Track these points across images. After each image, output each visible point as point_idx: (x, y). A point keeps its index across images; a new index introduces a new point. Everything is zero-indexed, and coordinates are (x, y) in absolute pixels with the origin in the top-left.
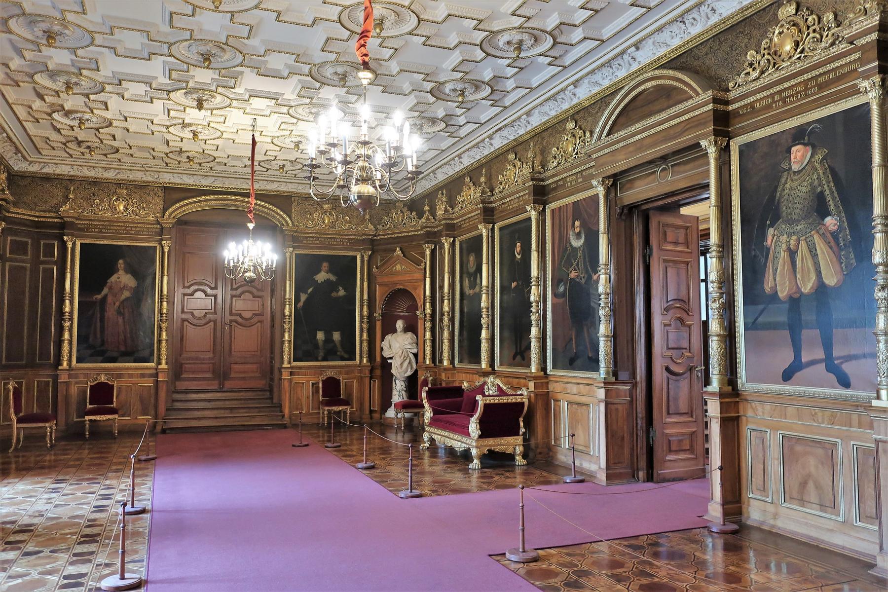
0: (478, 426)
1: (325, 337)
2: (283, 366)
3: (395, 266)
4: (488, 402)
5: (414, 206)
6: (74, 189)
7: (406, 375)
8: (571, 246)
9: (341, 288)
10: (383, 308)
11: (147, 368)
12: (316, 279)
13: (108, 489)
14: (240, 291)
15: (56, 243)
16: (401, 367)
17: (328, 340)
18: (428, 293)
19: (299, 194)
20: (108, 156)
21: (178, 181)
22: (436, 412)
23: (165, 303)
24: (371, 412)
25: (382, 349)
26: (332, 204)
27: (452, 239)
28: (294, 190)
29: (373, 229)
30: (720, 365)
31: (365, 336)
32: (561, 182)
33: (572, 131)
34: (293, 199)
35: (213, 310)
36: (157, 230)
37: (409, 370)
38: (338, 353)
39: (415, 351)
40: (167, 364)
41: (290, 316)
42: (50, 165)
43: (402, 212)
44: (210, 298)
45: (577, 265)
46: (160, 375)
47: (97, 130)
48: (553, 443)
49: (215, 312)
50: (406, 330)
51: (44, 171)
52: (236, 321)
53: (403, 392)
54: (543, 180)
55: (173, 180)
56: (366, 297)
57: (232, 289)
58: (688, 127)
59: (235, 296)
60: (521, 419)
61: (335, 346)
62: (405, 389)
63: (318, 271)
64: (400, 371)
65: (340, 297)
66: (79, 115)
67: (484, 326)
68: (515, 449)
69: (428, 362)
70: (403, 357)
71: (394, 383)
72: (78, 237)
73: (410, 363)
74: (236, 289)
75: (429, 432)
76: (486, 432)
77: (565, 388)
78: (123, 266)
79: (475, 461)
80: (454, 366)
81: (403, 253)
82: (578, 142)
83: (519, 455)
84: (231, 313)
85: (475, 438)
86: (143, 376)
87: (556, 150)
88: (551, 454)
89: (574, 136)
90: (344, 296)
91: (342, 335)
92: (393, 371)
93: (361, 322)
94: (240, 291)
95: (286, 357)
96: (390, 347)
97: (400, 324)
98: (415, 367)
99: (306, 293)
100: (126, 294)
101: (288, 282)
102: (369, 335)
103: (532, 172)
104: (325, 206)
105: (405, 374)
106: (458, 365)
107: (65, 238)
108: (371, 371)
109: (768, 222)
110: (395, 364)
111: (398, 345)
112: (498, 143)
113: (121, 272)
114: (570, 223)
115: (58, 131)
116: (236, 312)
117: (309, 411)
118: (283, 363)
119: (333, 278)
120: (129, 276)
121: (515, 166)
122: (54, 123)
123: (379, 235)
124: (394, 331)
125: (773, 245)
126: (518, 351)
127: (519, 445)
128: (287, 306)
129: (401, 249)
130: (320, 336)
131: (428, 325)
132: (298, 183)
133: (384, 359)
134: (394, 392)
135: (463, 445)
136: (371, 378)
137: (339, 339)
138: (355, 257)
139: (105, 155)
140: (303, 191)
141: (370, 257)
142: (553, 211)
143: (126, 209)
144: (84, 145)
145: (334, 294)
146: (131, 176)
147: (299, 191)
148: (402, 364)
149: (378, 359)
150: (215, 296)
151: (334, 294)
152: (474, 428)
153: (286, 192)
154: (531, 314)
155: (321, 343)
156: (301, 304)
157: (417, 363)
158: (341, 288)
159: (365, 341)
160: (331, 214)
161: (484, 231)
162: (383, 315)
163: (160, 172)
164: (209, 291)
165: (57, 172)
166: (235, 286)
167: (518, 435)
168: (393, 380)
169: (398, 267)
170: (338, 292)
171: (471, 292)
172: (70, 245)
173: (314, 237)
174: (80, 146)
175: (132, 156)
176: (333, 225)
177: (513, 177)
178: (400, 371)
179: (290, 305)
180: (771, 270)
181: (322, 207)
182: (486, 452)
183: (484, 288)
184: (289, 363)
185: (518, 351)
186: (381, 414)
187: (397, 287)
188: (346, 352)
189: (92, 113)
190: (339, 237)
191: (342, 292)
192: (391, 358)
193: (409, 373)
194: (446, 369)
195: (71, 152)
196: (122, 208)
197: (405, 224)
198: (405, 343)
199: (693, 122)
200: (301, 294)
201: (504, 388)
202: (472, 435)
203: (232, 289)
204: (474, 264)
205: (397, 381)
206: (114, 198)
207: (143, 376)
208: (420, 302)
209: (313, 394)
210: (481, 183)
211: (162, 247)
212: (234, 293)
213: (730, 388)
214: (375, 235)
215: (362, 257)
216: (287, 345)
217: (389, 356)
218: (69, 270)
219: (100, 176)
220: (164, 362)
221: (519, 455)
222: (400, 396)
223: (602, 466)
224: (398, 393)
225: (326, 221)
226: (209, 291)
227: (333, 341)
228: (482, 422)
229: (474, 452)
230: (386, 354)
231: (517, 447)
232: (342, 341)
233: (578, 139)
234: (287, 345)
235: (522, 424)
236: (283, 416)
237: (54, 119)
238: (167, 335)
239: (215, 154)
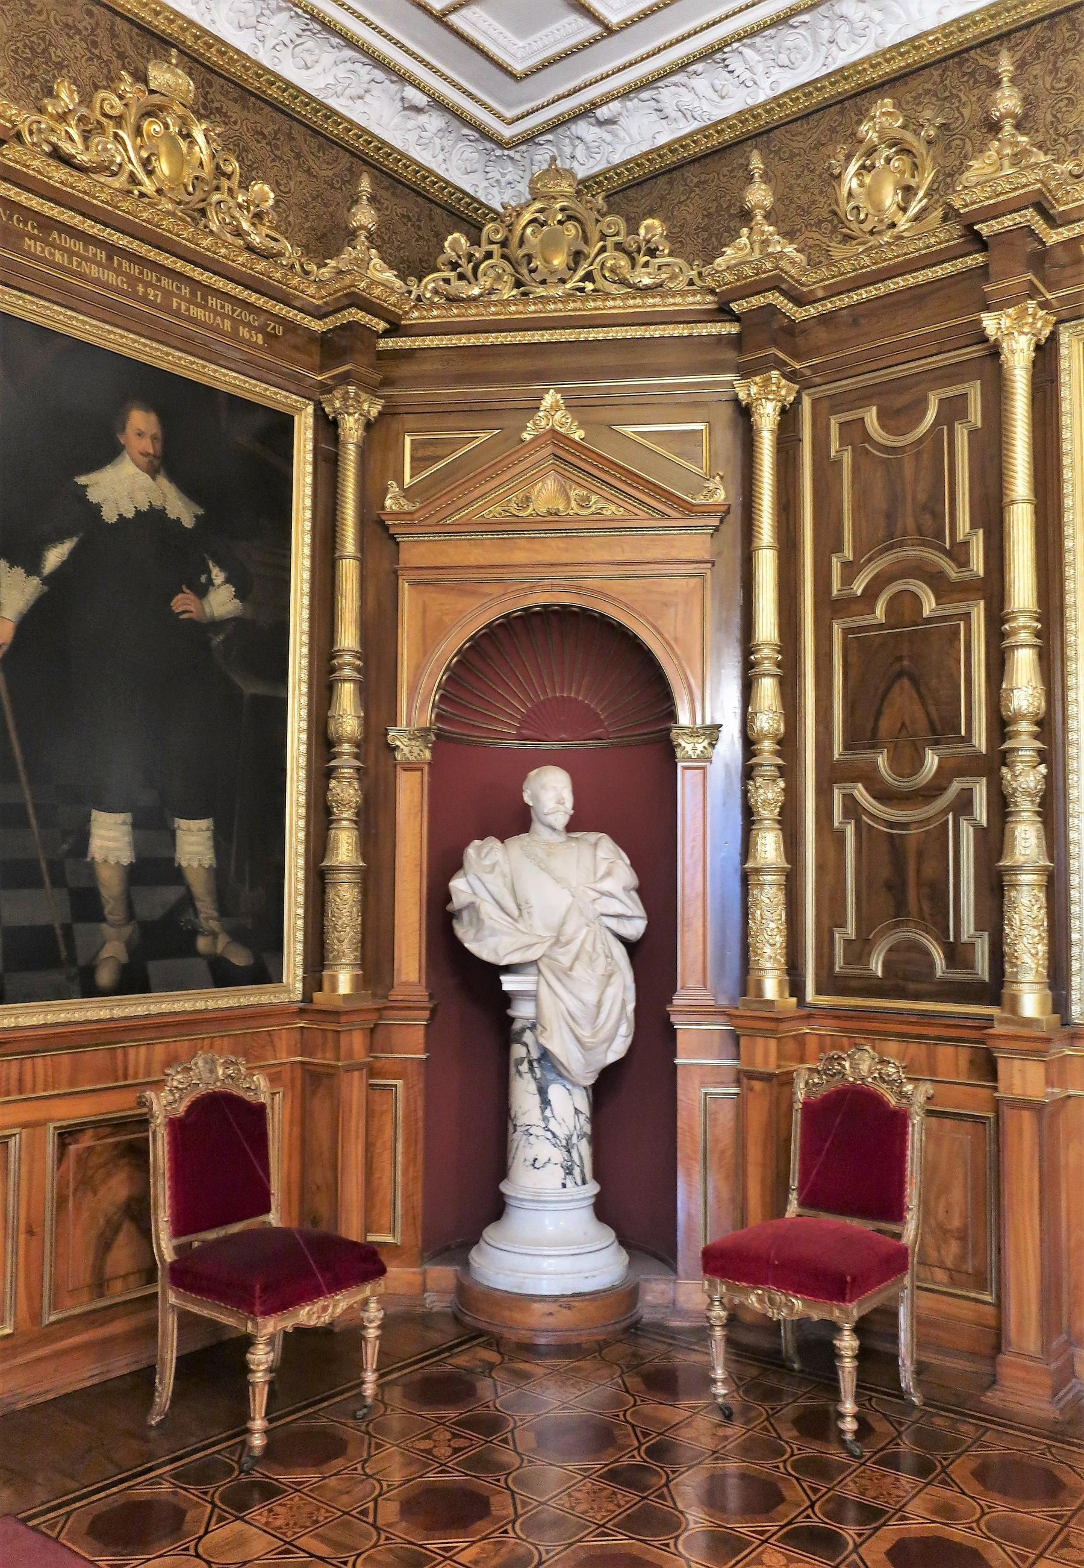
1: (137, 846)
12: (93, 496)
38: (202, 944)
61: (189, 900)
65: (217, 625)
69: (771, 988)
90: (235, 622)
91: (221, 840)
99: (32, 566)
117: (36, 1317)
137: (208, 858)
138: (283, 425)
145: (183, 603)
151: (183, 603)
155: (110, 884)
158: (218, 575)
170: (202, 591)
188: (237, 936)
190: (220, 283)
198: (607, 885)
209: (61, 1202)
222: (569, 1171)
224: (558, 1155)
227: (176, 875)
232: (218, 874)
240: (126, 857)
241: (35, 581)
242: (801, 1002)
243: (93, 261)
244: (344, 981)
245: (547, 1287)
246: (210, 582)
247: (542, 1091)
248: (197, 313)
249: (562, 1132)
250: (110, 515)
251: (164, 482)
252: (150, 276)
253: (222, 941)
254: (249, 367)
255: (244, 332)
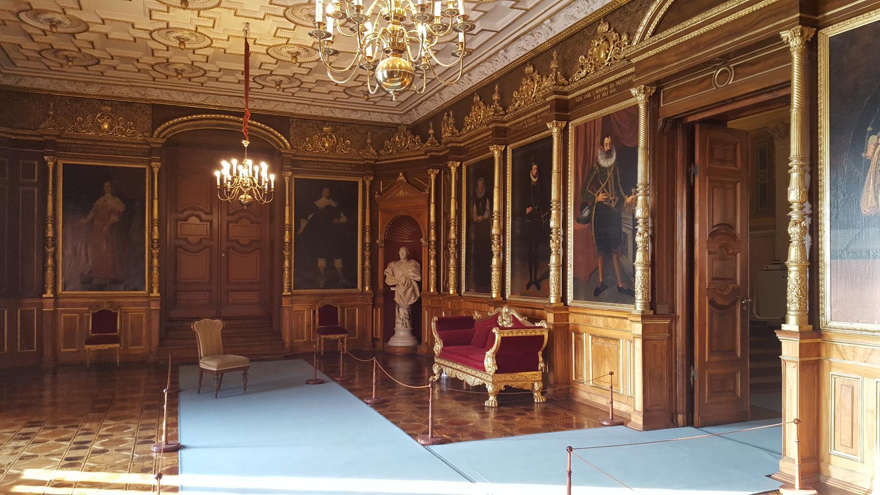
0: (495, 362)
2: (283, 294)
3: (398, 192)
4: (506, 335)
5: (418, 129)
6: (54, 105)
7: (409, 303)
8: (599, 166)
9: (342, 215)
10: (385, 235)
11: (138, 297)
12: (317, 205)
13: (86, 434)
14: (236, 216)
15: (36, 163)
16: (405, 296)
17: (330, 267)
18: (432, 219)
19: (297, 115)
20: (90, 68)
21: (167, 98)
22: (445, 344)
23: (156, 228)
24: (373, 339)
25: (385, 277)
26: (332, 126)
27: (459, 163)
28: (292, 111)
29: (375, 153)
30: (800, 300)
31: (367, 263)
32: (589, 95)
33: (604, 35)
34: (291, 120)
35: (208, 236)
36: (146, 151)
37: (413, 298)
38: (340, 281)
39: (418, 278)
40: (159, 291)
41: (290, 243)
42: (26, 78)
43: (405, 136)
44: (206, 223)
45: (607, 187)
46: (152, 303)
47: (73, 35)
48: (574, 379)
49: (211, 239)
50: (409, 258)
51: (21, 84)
52: (233, 248)
53: (407, 320)
54: (566, 94)
55: (161, 98)
56: (367, 223)
57: (228, 214)
58: (763, 16)
59: (232, 222)
60: (540, 353)
62: (408, 317)
63: (319, 197)
64: (404, 299)
66: (49, 16)
67: (495, 254)
68: (533, 385)
69: (432, 290)
70: (406, 285)
71: (397, 311)
72: (60, 157)
73: (413, 291)
74: (233, 214)
75: (439, 364)
76: (503, 367)
77: (589, 321)
78: (109, 188)
79: (491, 398)
80: (460, 295)
81: (406, 179)
82: (612, 47)
83: (537, 392)
84: (228, 240)
85: (491, 374)
86: (134, 304)
87: (584, 58)
88: (571, 390)
89: (606, 40)
92: (397, 299)
93: (363, 249)
94: (236, 216)
95: (286, 285)
96: (393, 275)
97: (403, 252)
98: (418, 294)
99: (306, 219)
100: (114, 218)
101: (287, 208)
102: (371, 263)
103: (555, 84)
104: (325, 129)
105: (408, 302)
106: (464, 293)
107: (46, 158)
108: (374, 299)
109: (869, 129)
110: (399, 291)
111: (401, 273)
112: (514, 54)
113: (107, 195)
114: (598, 140)
115: (30, 36)
116: (233, 238)
118: (283, 291)
119: (333, 204)
120: (117, 199)
121: (533, 80)
122: (24, 26)
123: (381, 160)
124: (397, 258)
125: (876, 156)
126: (533, 280)
127: (538, 381)
128: (287, 232)
129: (404, 175)
130: (322, 263)
131: (433, 253)
132: (296, 103)
133: (387, 287)
134: (398, 320)
135: (478, 380)
136: (373, 306)
137: (341, 266)
139: (86, 67)
140: (302, 112)
141: (372, 182)
142: (577, 128)
143: (111, 127)
144: (61, 54)
145: (335, 221)
146: (116, 92)
147: (297, 112)
148: (405, 292)
149: (381, 286)
150: (211, 222)
151: (335, 221)
152: (489, 362)
153: (284, 113)
154: (551, 241)
156: (301, 230)
157: (420, 290)
158: (342, 215)
159: (367, 269)
160: (331, 137)
161: (496, 153)
162: (386, 242)
163: (146, 87)
164: (204, 216)
165: (35, 86)
166: (231, 212)
167: (537, 370)
168: (397, 309)
169: (401, 193)
171: (480, 218)
172: (51, 164)
173: (314, 161)
174: (56, 56)
175: (115, 68)
176: (333, 148)
177: (530, 93)
178: (404, 299)
179: (290, 231)
180: (871, 187)
181: (322, 130)
182: (503, 388)
183: (496, 214)
184: (290, 290)
185: (533, 280)
186: (384, 342)
187: (401, 214)
189: (65, 13)
191: (343, 219)
192: (394, 286)
193: (413, 301)
194: (452, 297)
195: (48, 63)
196: (106, 126)
197: (408, 148)
199: (771, 10)
200: (301, 220)
201: (520, 319)
202: (488, 370)
203: (228, 214)
204: (483, 189)
205: (401, 310)
206: (99, 115)
207: (134, 304)
208: (424, 229)
210: (494, 101)
211: (151, 169)
212: (230, 218)
213: (811, 326)
214: (377, 160)
215: (364, 183)
216: (287, 272)
217: (391, 284)
218: (50, 192)
219: (82, 90)
220: (155, 290)
221: (537, 392)
222: (403, 325)
223: (637, 409)
224: (401, 321)
225: (327, 145)
226: (204, 216)
228: (498, 357)
229: (490, 388)
230: (389, 281)
231: (536, 384)
233: (612, 43)
234: (287, 272)
235: (541, 359)
236: (284, 344)
237: (21, 21)
238: (159, 262)
239: (207, 67)
240: (325, 266)
241: (307, 221)
242: (439, 293)
243: (315, 165)
244: (367, 289)
245: (399, 345)
246: (340, 216)
247: (398, 309)
248: (336, 168)
249: (401, 317)
250: (320, 208)
251: (330, 200)
252: (326, 164)
253: (344, 281)
254: (347, 175)
255: (346, 168)
